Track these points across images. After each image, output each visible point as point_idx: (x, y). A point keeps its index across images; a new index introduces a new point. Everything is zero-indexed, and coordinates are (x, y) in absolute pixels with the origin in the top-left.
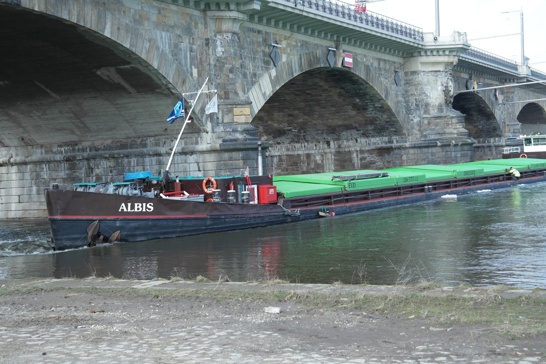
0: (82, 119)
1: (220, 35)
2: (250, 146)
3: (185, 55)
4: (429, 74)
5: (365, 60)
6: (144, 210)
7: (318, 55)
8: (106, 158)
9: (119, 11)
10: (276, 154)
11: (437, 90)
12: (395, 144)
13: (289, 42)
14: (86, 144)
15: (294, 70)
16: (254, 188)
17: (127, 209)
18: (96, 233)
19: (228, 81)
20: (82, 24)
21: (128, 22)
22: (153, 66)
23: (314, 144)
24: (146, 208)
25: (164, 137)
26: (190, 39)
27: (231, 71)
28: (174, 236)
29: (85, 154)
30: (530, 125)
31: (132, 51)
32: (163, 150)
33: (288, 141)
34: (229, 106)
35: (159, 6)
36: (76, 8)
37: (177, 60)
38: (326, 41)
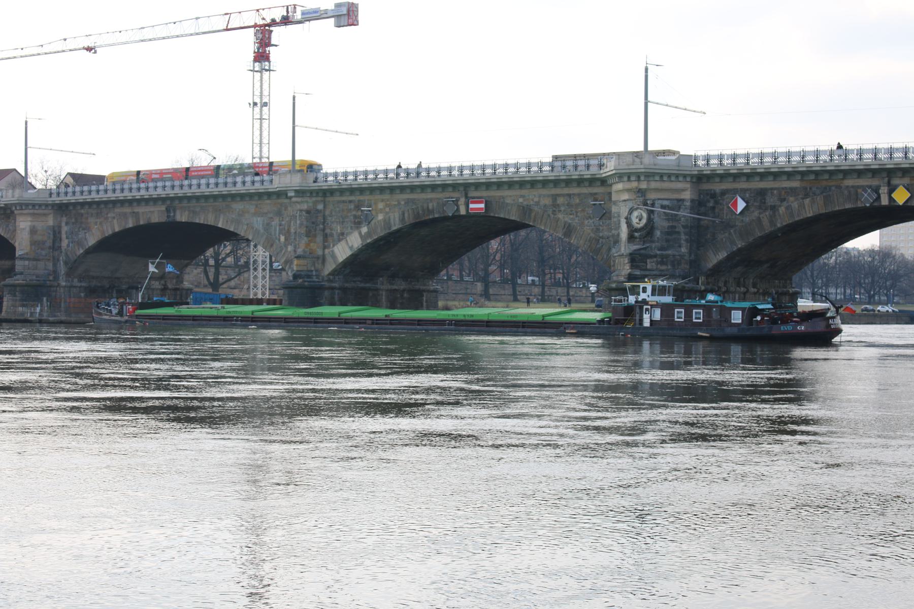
7: (430, 207)
13: (388, 203)
15: (393, 223)
20: (206, 223)
21: (234, 216)
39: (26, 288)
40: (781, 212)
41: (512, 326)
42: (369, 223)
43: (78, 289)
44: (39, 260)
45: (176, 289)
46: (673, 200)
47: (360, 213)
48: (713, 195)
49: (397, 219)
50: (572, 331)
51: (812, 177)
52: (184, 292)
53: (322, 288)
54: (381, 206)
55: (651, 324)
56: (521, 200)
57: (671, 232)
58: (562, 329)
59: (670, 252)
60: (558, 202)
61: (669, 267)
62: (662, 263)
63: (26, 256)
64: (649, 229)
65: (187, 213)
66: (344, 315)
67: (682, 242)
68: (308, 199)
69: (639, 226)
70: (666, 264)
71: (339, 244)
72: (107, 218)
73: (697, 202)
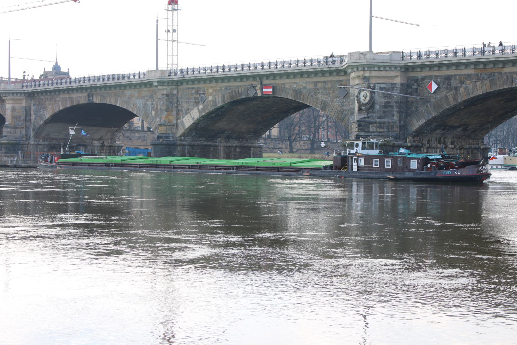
7: (240, 92)
9: (123, 96)
13: (215, 89)
20: (110, 104)
21: (126, 99)
37: (145, 109)
38: (248, 82)
39: (8, 145)
40: (461, 91)
41: (271, 171)
42: (204, 102)
43: (42, 146)
44: (17, 128)
45: (110, 146)
46: (389, 84)
47: (198, 96)
48: (416, 81)
49: (220, 100)
50: (307, 174)
51: (482, 66)
52: (116, 148)
53: (175, 145)
54: (210, 91)
55: (358, 170)
56: (295, 86)
57: (387, 105)
58: (301, 172)
59: (386, 120)
60: (318, 87)
61: (385, 130)
62: (380, 127)
63: (9, 126)
64: (371, 104)
65: (99, 97)
66: (173, 163)
67: (395, 113)
68: (167, 87)
69: (365, 102)
70: (383, 128)
71: (186, 116)
72: (55, 101)
73: (406, 86)
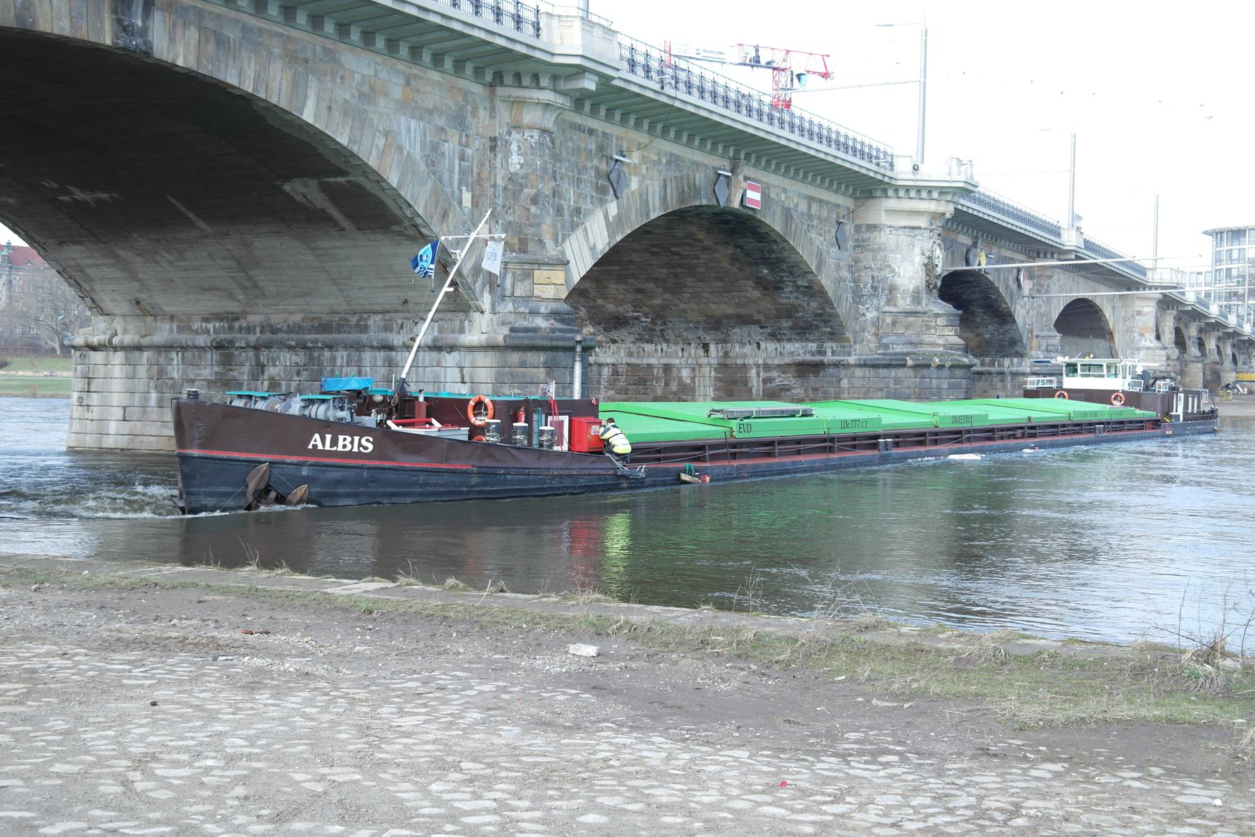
0: (251, 273)
1: (518, 133)
2: (560, 343)
3: (449, 164)
4: (899, 232)
5: (783, 198)
6: (355, 449)
7: (697, 182)
8: (290, 348)
10: (609, 361)
11: (913, 263)
12: (829, 358)
13: (646, 154)
14: (254, 319)
15: (651, 207)
16: (562, 422)
17: (324, 445)
18: (262, 486)
19: (528, 220)
20: (262, 95)
21: (347, 97)
22: (390, 181)
23: (679, 348)
24: (360, 445)
25: (402, 315)
26: (461, 137)
27: (534, 201)
28: (408, 500)
29: (252, 339)
30: (1076, 339)
31: (351, 152)
32: (397, 339)
33: (632, 338)
34: (527, 267)
35: (408, 70)
36: (252, 65)
37: (434, 174)
38: (713, 157)
